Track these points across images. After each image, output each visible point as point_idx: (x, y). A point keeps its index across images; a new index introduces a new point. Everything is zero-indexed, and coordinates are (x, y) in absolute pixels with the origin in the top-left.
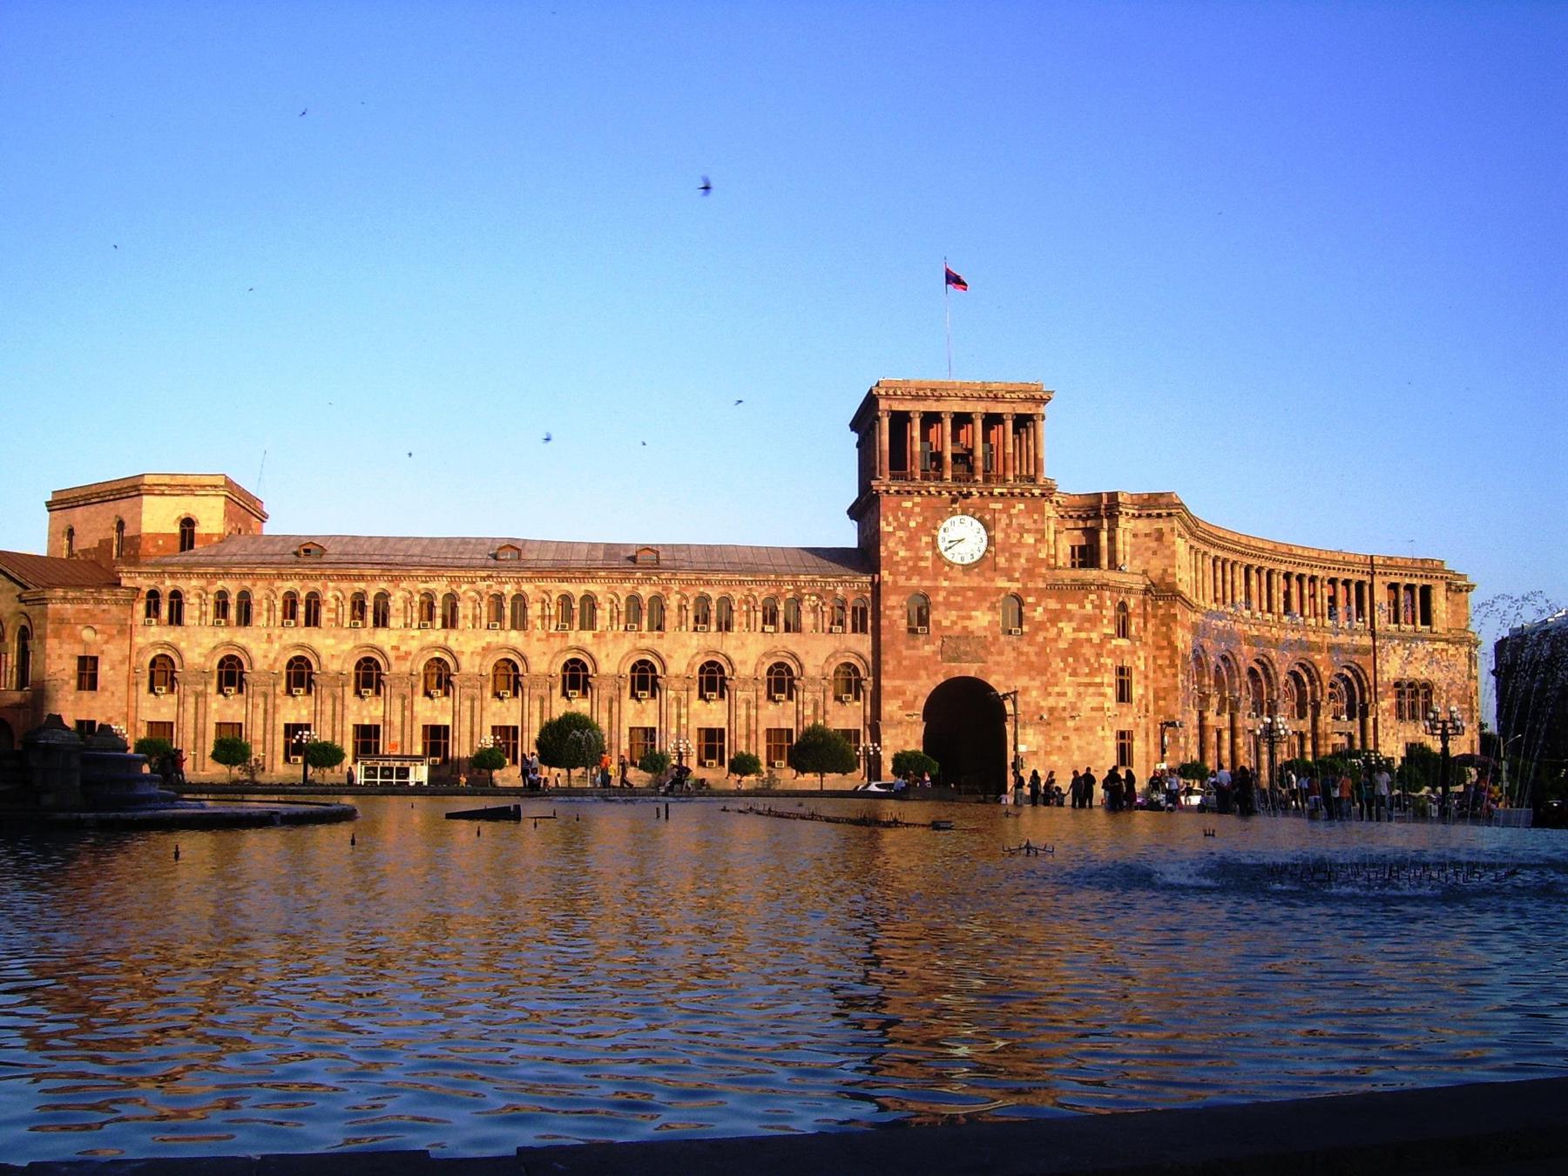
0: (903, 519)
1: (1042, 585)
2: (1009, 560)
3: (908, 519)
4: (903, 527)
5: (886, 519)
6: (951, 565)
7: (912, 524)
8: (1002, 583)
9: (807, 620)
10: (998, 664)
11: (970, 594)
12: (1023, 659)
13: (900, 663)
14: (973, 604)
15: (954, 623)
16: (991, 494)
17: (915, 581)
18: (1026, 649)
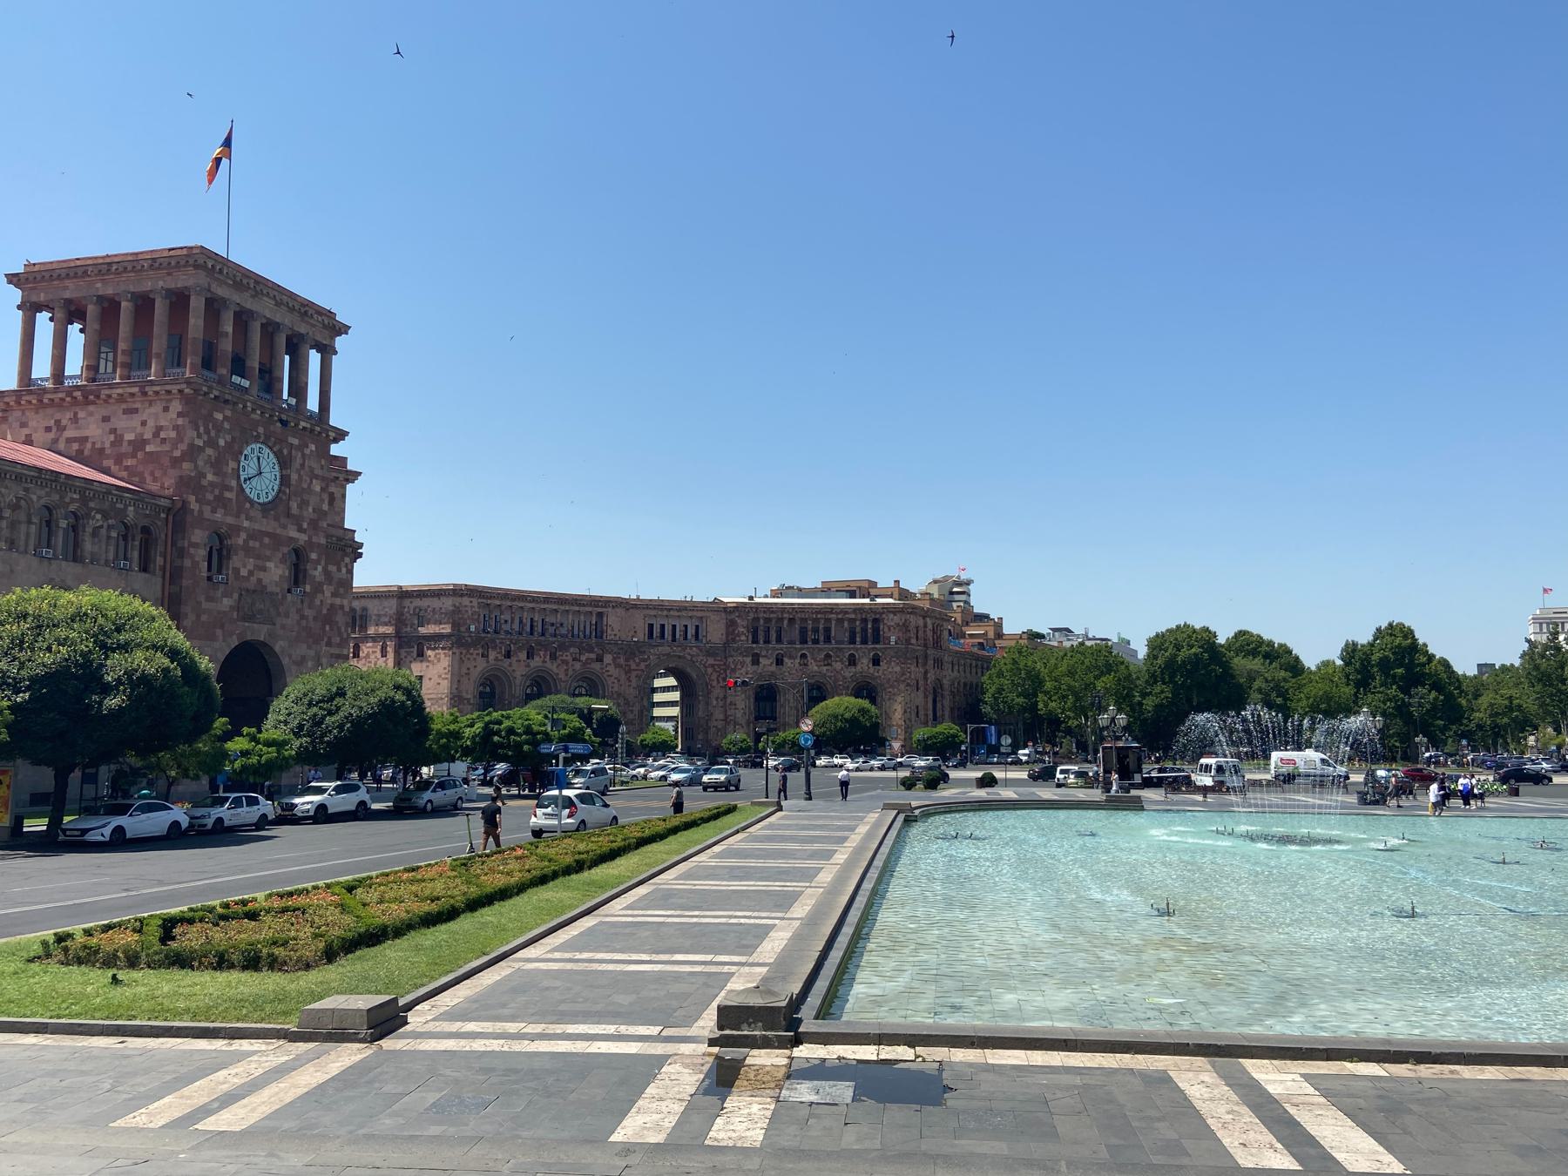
0: (213, 434)
1: (323, 541)
2: (300, 507)
3: (218, 436)
4: (212, 443)
5: (197, 429)
6: (251, 502)
7: (222, 442)
8: (294, 534)
9: (88, 546)
10: (283, 627)
11: (266, 540)
12: (304, 623)
13: (198, 616)
14: (268, 553)
15: (251, 573)
16: (297, 425)
17: (218, 516)
18: (307, 612)
